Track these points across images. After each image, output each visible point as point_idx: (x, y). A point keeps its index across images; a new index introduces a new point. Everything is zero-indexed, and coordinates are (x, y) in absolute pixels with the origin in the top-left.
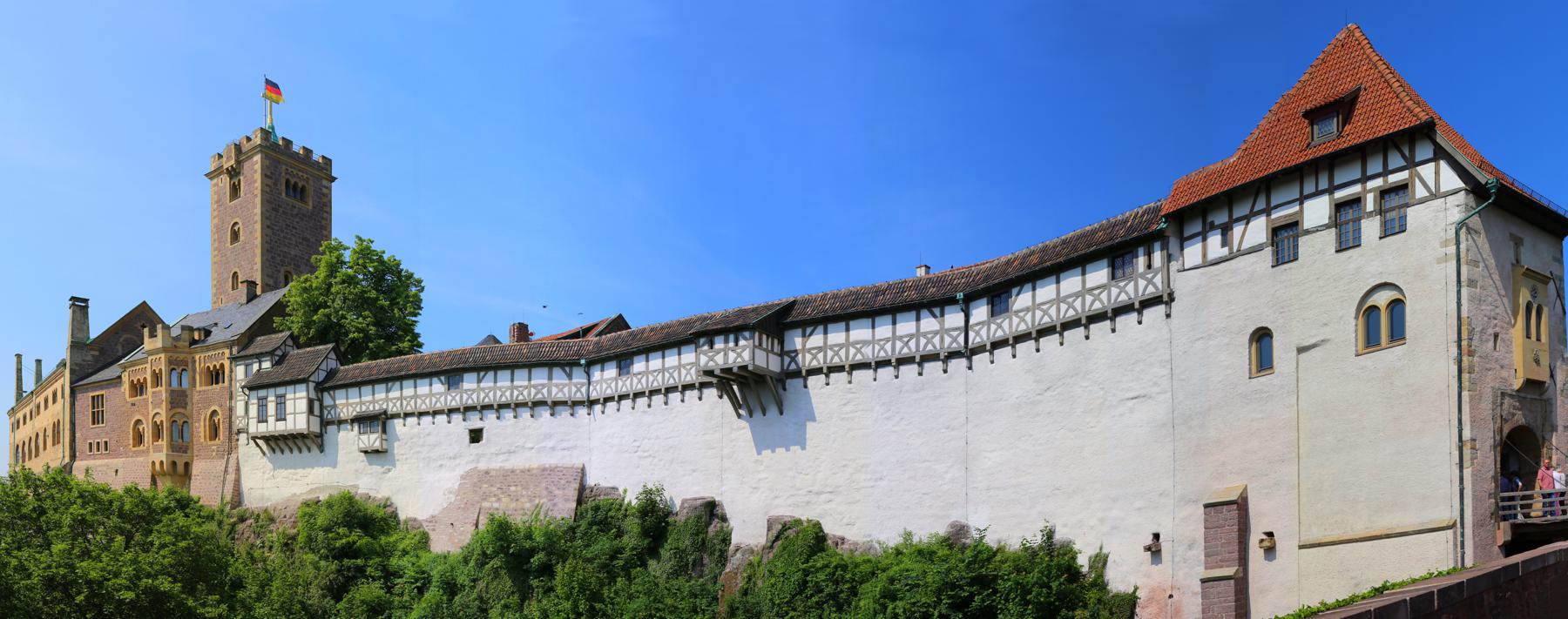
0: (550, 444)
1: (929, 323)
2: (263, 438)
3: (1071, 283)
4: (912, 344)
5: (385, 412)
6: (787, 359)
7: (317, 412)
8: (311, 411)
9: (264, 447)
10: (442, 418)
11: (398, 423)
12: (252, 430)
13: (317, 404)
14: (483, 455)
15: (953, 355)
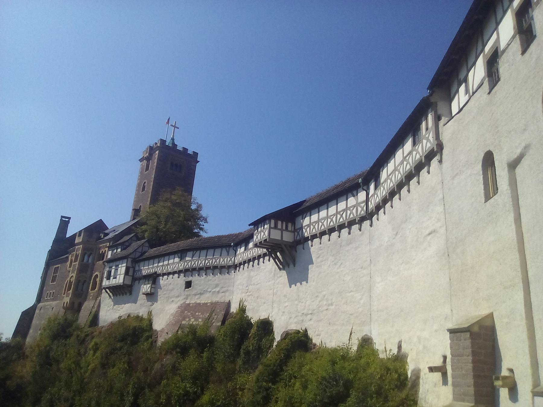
0: (217, 289)
1: (352, 201)
2: (107, 288)
3: (399, 155)
4: (344, 215)
5: (156, 273)
6: (296, 234)
7: (131, 273)
8: (127, 273)
9: (111, 294)
10: (176, 275)
11: (161, 278)
12: (104, 284)
13: (131, 271)
14: (190, 295)
15: (362, 219)
